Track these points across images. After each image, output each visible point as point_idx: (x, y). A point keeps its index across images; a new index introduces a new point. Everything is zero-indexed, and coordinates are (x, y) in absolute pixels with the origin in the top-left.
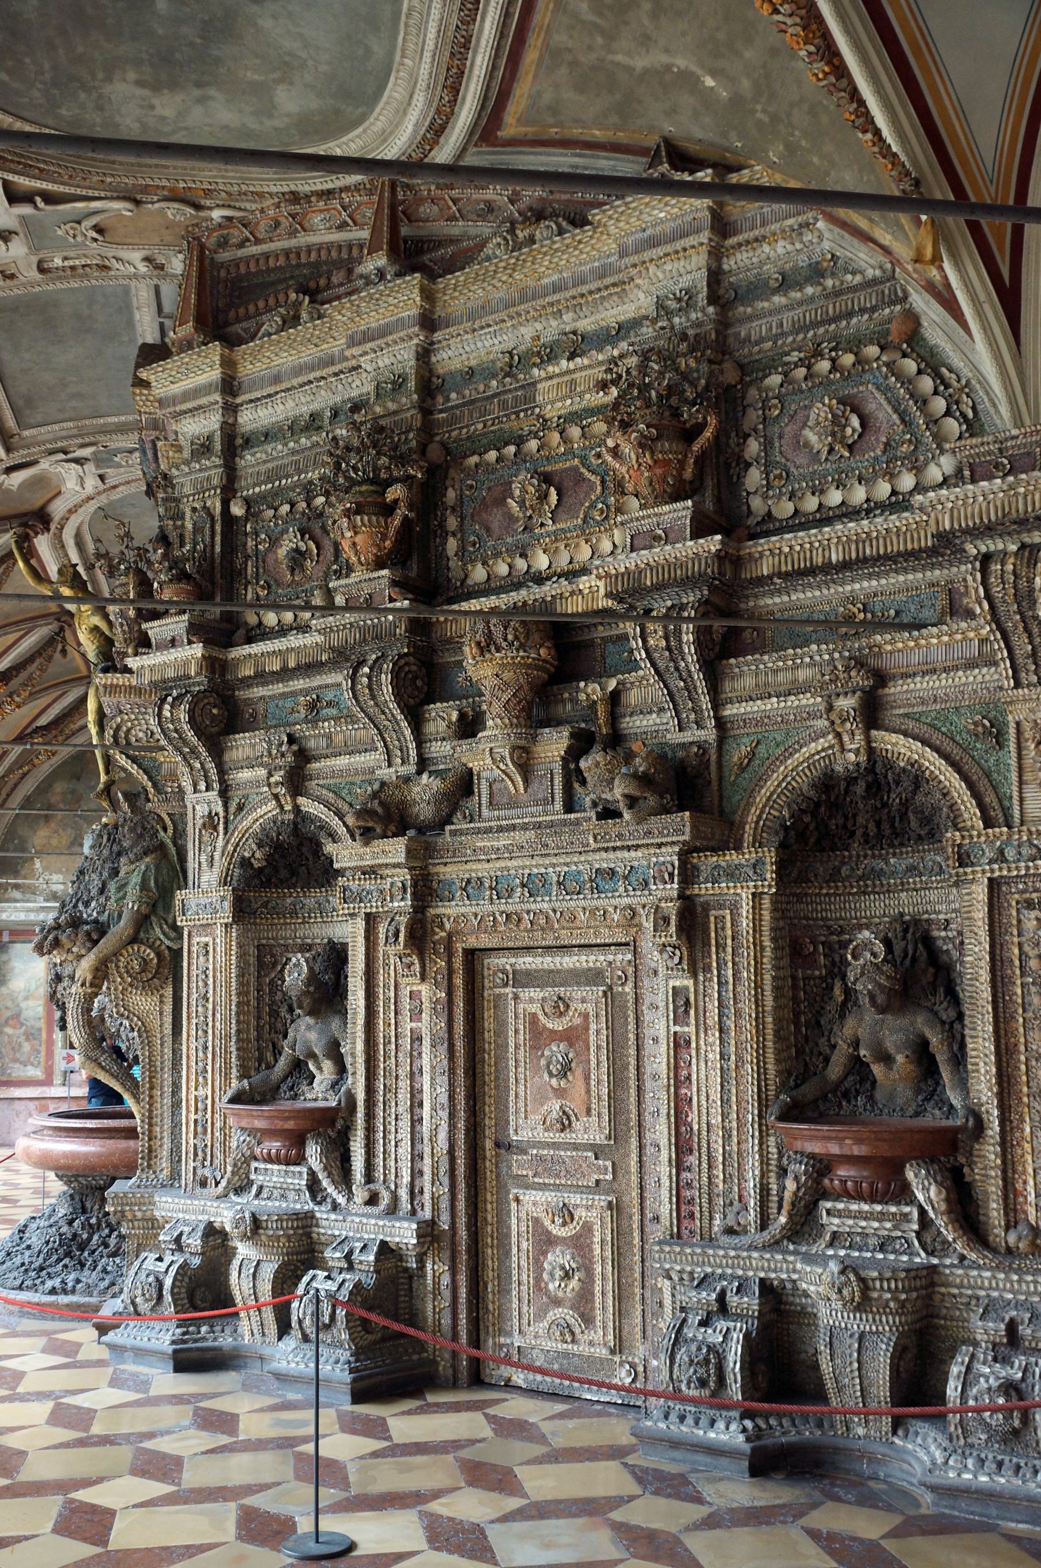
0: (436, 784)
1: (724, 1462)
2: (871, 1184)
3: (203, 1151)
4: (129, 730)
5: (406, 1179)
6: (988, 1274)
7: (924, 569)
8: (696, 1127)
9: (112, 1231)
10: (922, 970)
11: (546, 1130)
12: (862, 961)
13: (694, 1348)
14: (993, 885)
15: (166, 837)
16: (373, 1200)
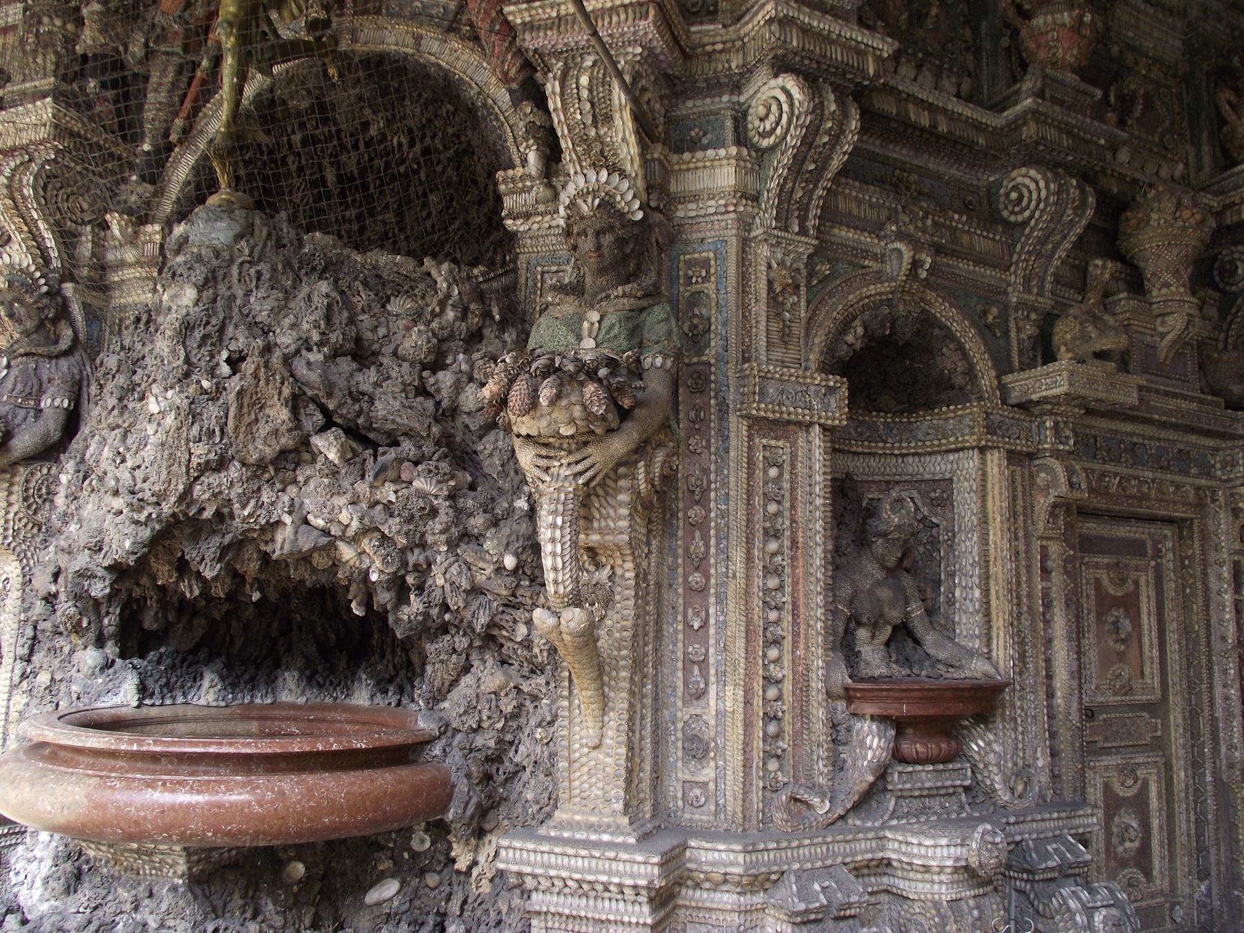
11: (1115, 694)
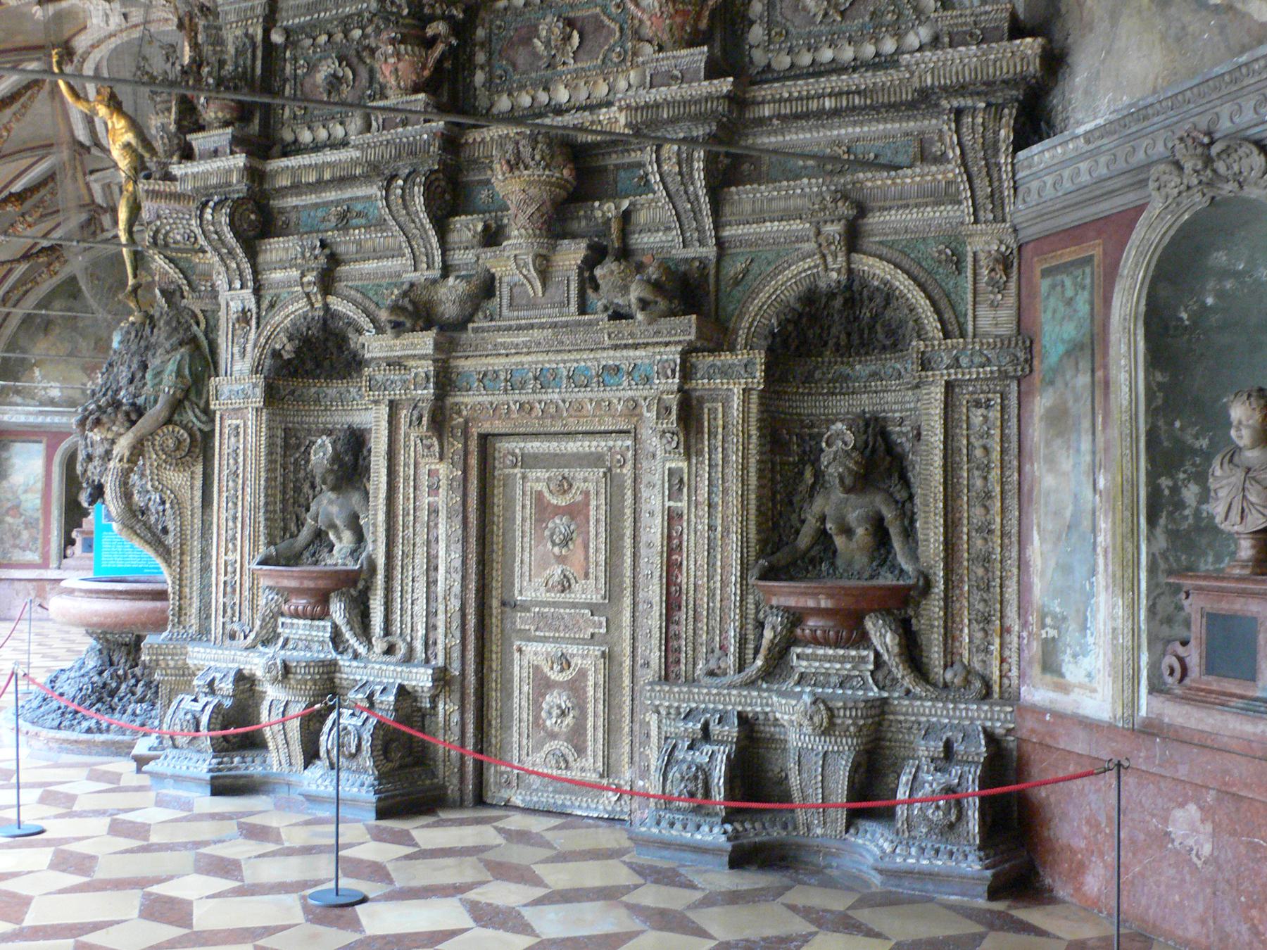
0: (462, 287)
1: (709, 858)
2: (837, 633)
3: (232, 608)
4: (167, 233)
5: (421, 631)
6: (929, 704)
7: (901, 120)
8: (684, 587)
9: (138, 681)
10: (882, 460)
12: (834, 448)
13: (685, 767)
14: (949, 386)
15: (199, 331)
16: (390, 650)
